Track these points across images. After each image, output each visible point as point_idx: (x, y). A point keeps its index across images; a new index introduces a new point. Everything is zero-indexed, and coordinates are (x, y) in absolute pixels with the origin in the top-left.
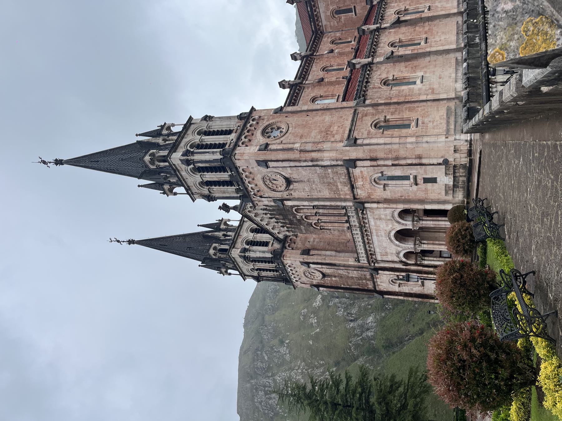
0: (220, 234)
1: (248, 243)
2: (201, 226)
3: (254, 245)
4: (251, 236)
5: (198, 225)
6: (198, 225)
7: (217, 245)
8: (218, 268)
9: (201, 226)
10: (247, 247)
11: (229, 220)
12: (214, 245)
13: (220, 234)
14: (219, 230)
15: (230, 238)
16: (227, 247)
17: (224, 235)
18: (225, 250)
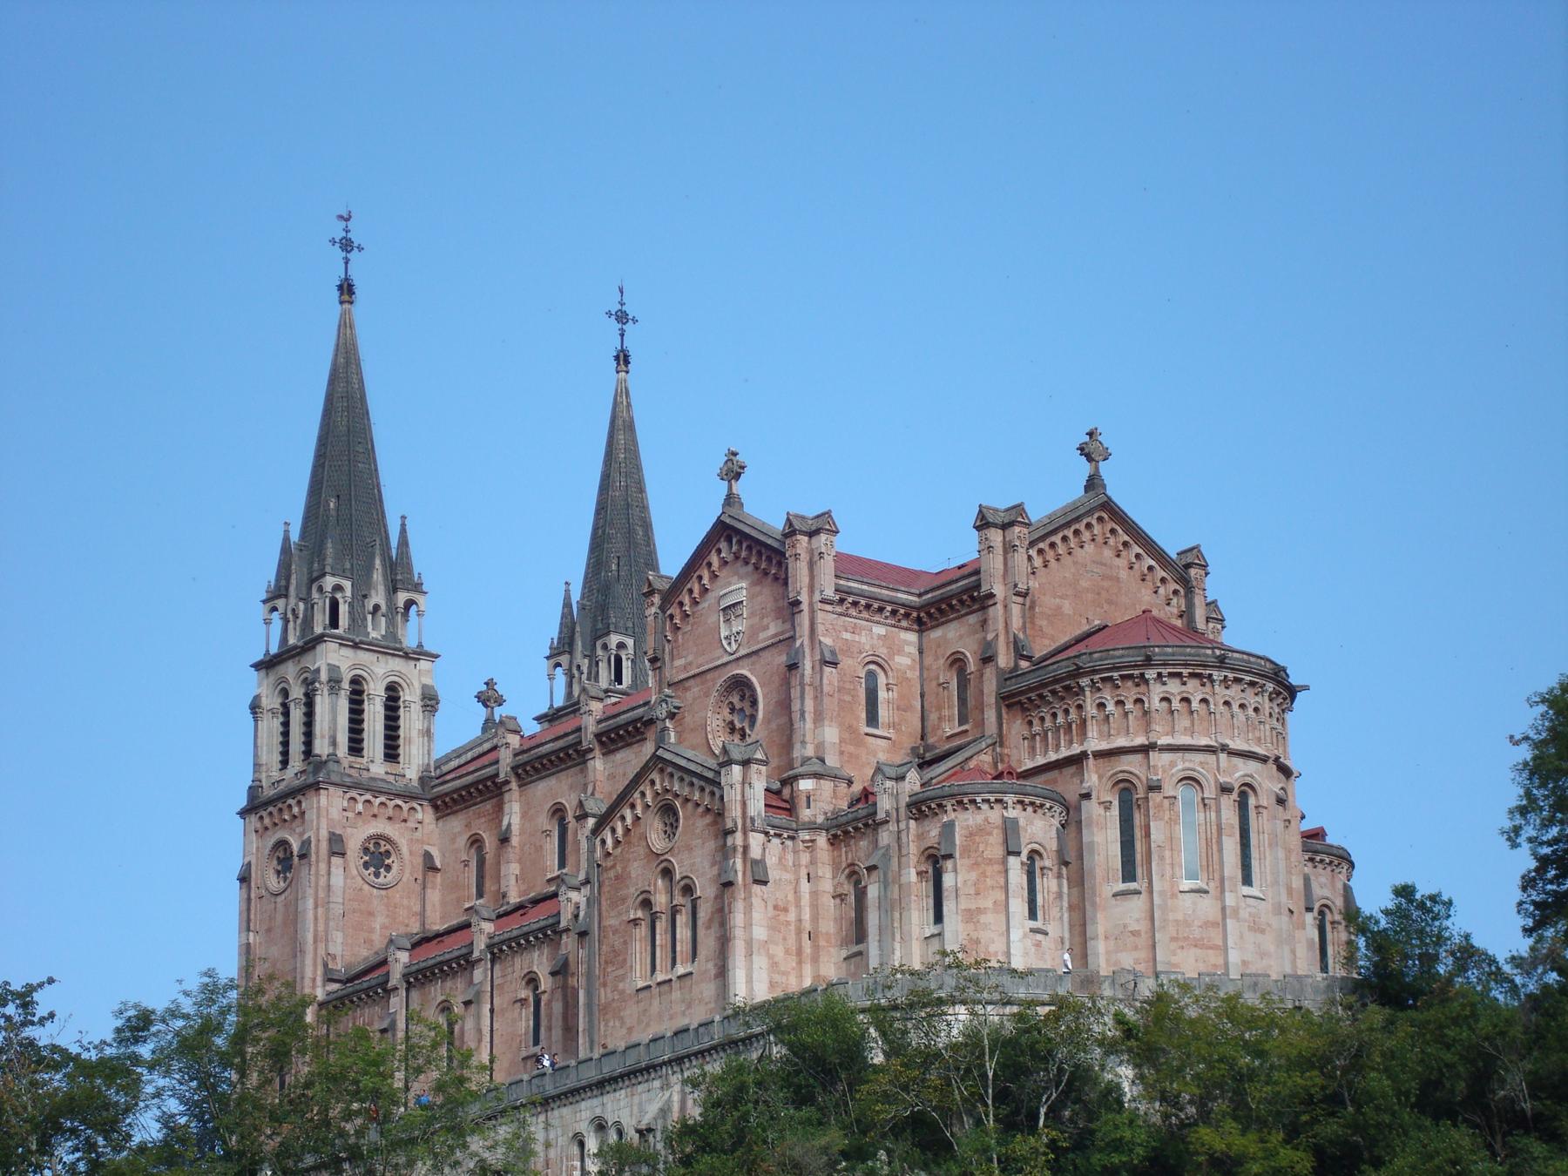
0: (378, 597)
1: (356, 681)
2: (403, 526)
3: (352, 701)
4: (376, 692)
5: (403, 517)
6: (403, 517)
7: (348, 593)
8: (287, 588)
9: (403, 526)
10: (346, 685)
11: (419, 614)
12: (347, 584)
13: (378, 597)
14: (393, 589)
15: (370, 629)
16: (344, 620)
17: (377, 608)
18: (334, 623)
